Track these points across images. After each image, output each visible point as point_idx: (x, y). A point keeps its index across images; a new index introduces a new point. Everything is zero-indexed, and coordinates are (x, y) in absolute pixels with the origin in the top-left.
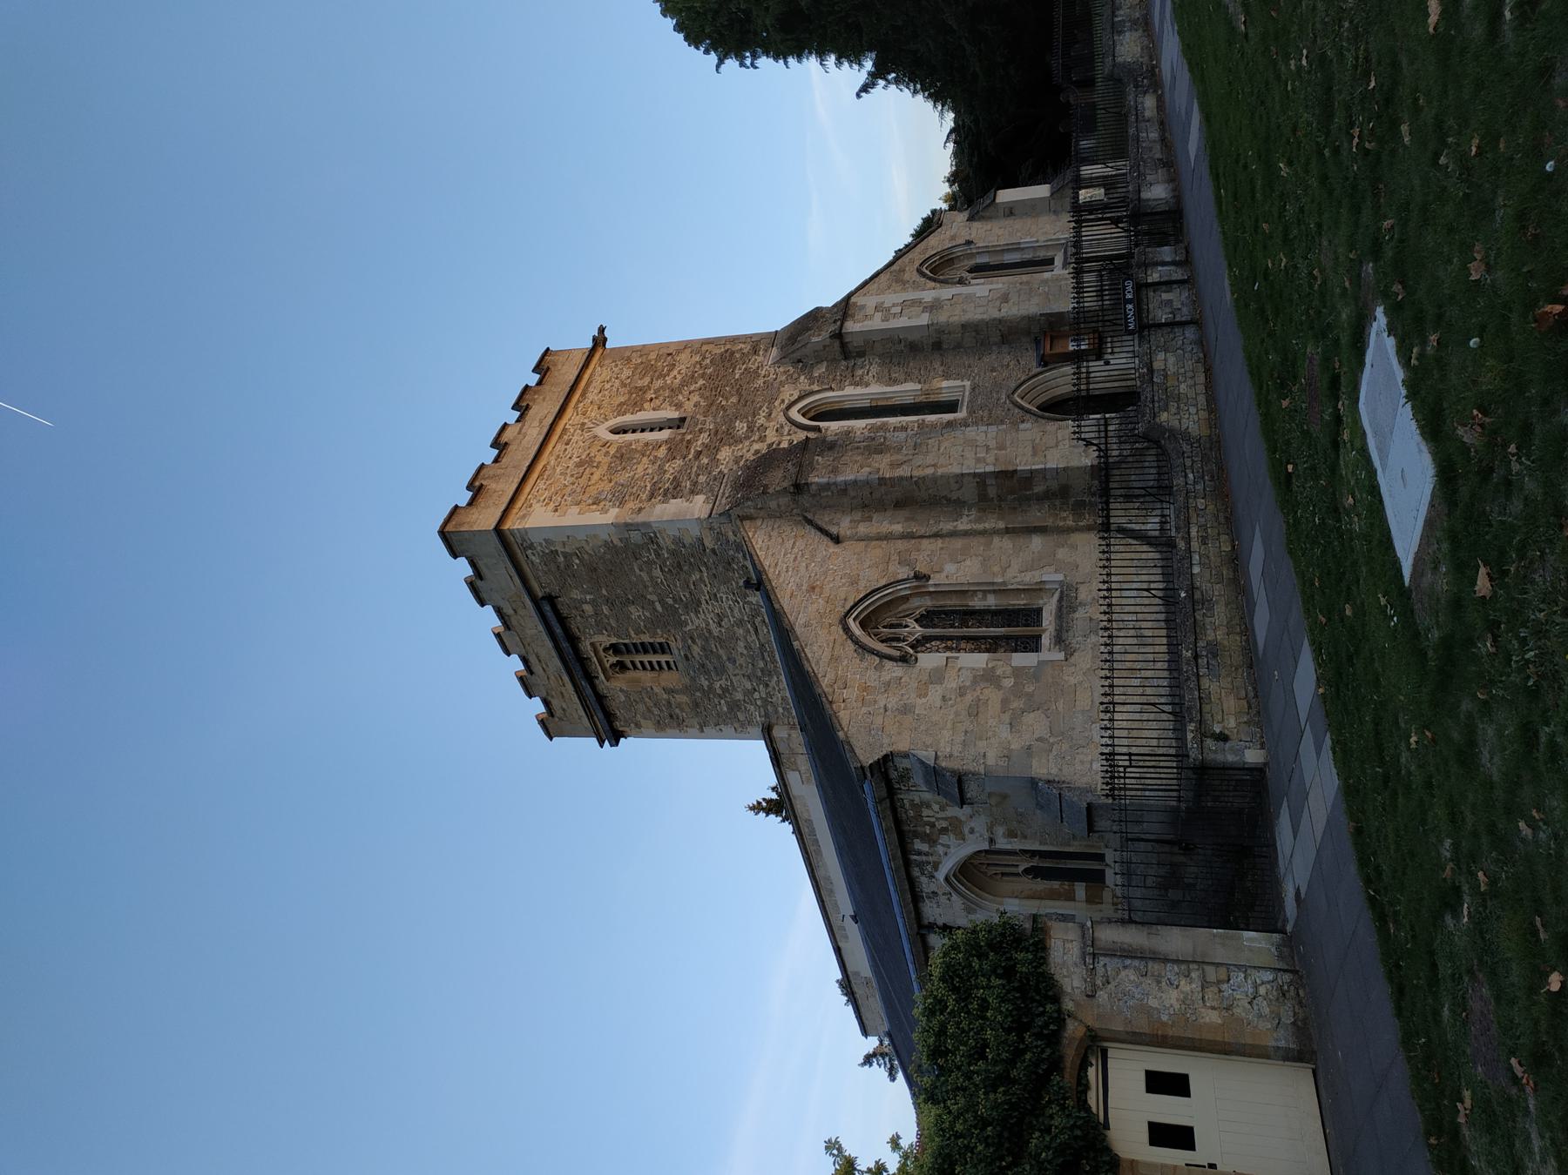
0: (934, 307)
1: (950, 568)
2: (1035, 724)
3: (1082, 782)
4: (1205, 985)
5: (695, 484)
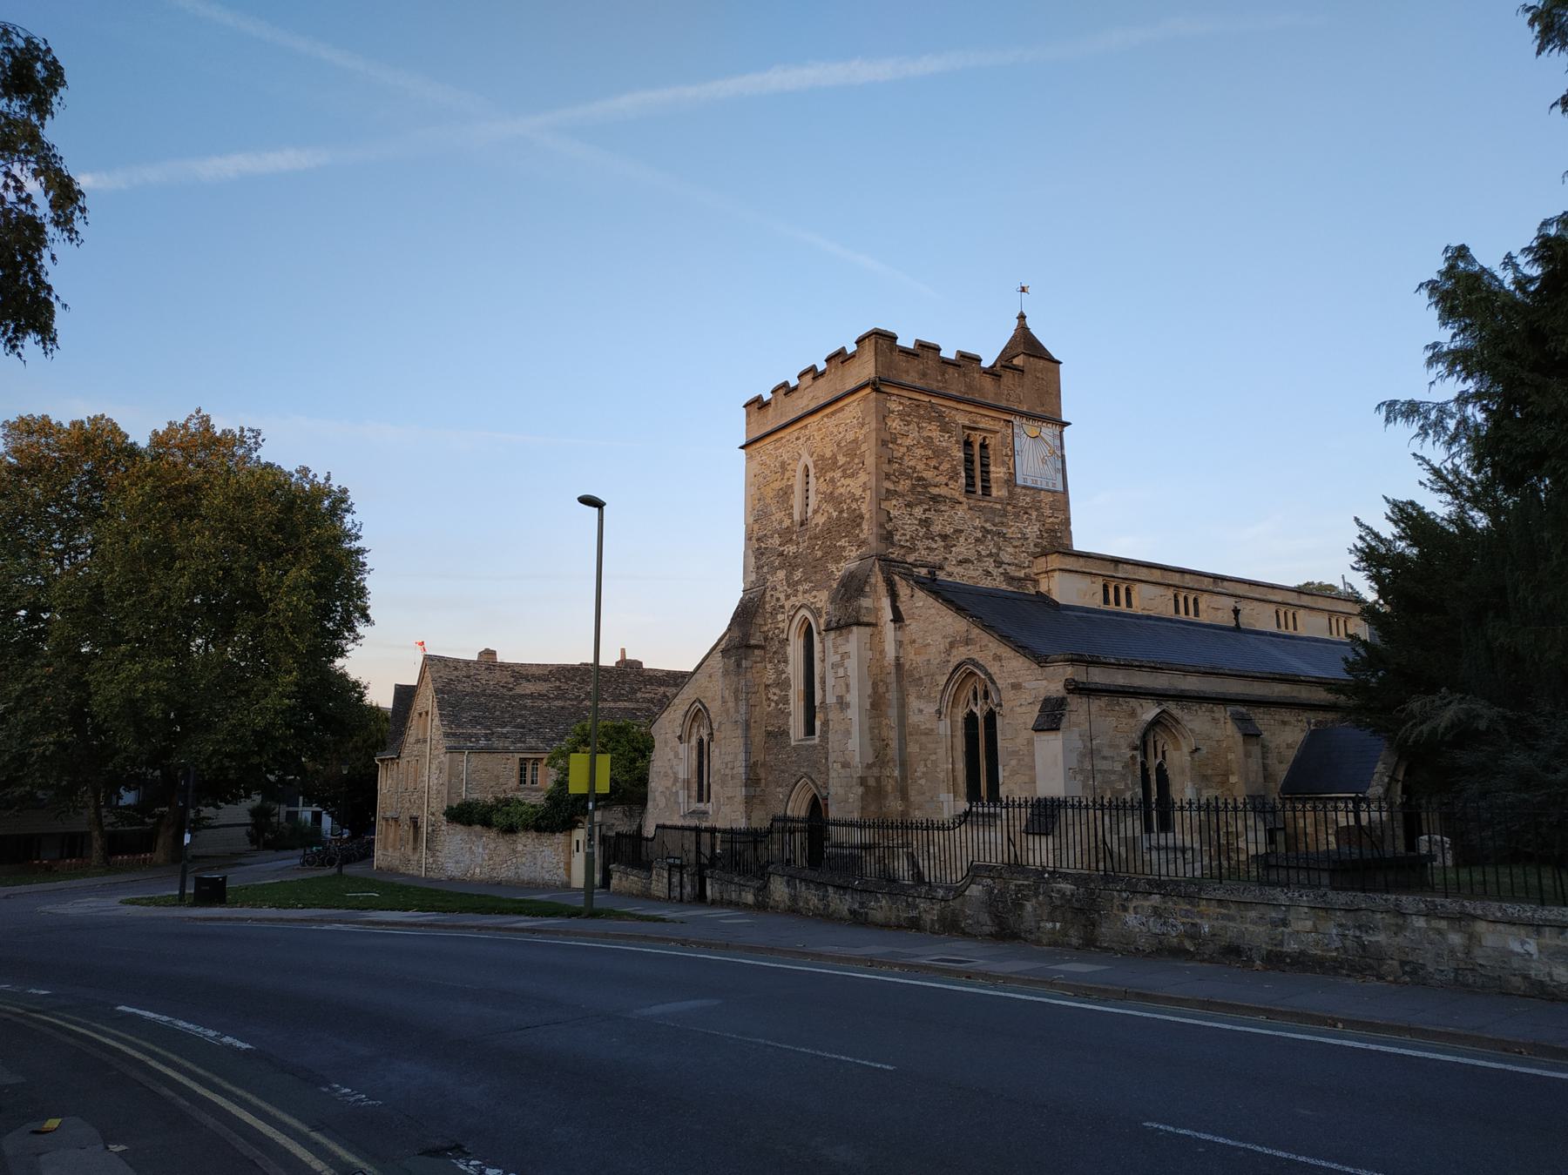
0: (842, 704)
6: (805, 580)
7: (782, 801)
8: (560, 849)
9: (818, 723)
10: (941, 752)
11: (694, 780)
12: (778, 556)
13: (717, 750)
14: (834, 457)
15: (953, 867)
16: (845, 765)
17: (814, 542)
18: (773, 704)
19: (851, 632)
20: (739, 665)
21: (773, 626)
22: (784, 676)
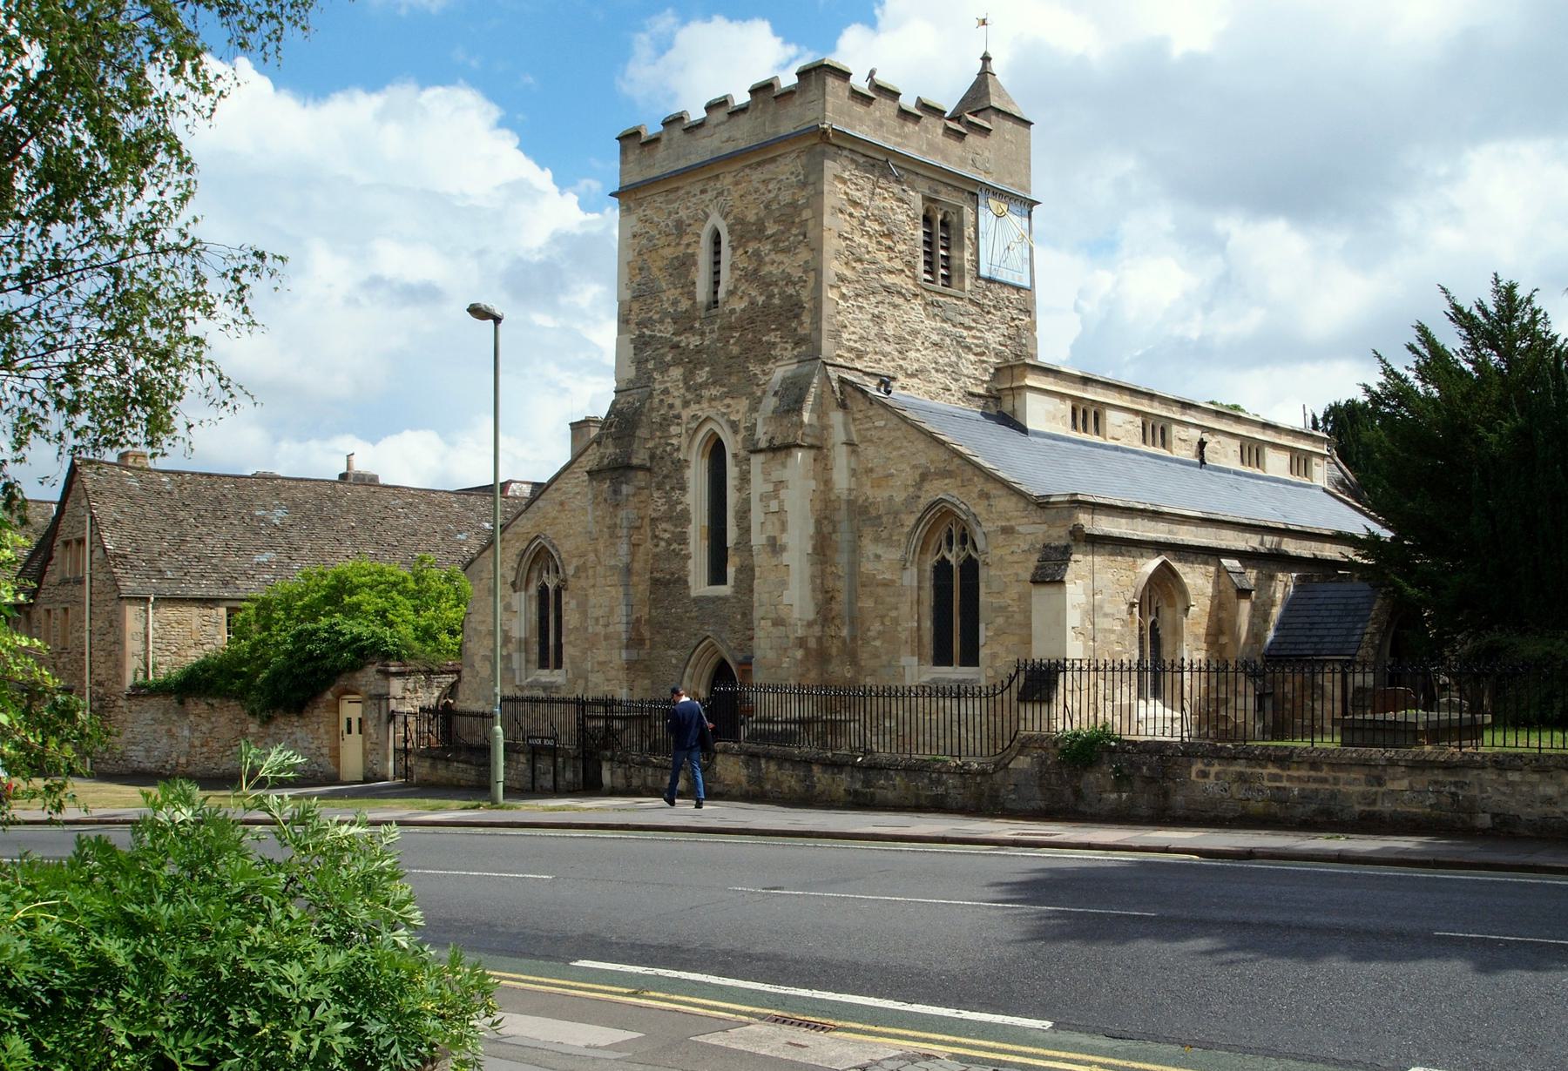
0: (775, 547)
6: (714, 383)
7: (676, 667)
8: (322, 730)
9: (731, 571)
10: (905, 608)
11: (535, 640)
12: (672, 348)
13: (573, 604)
14: (761, 228)
15: (914, 742)
16: (778, 622)
17: (727, 333)
18: (663, 544)
19: (788, 455)
20: (616, 492)
21: (662, 441)
22: (679, 508)
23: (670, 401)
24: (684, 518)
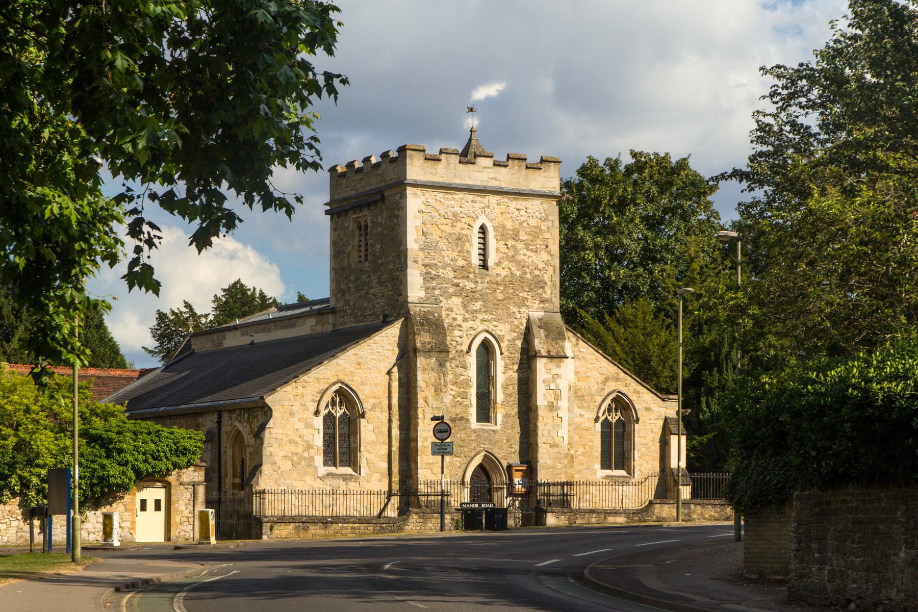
0: (552, 407)
1: (370, 427)
2: (286, 466)
3: (257, 483)
4: (188, 518)
5: (434, 289)
7: (459, 467)
20: (441, 365)
22: (462, 378)
23: (453, 315)
24: (467, 383)
